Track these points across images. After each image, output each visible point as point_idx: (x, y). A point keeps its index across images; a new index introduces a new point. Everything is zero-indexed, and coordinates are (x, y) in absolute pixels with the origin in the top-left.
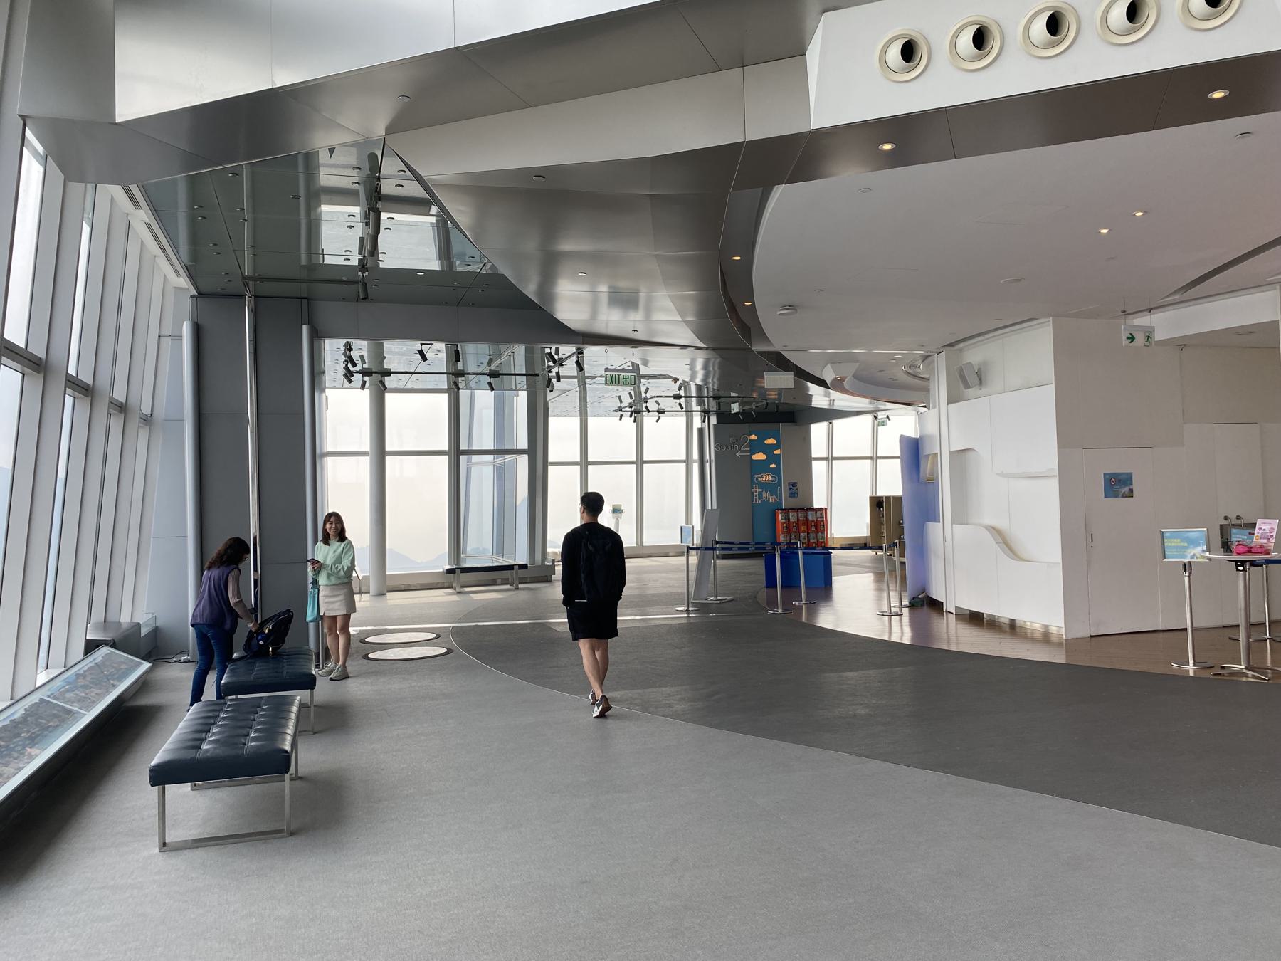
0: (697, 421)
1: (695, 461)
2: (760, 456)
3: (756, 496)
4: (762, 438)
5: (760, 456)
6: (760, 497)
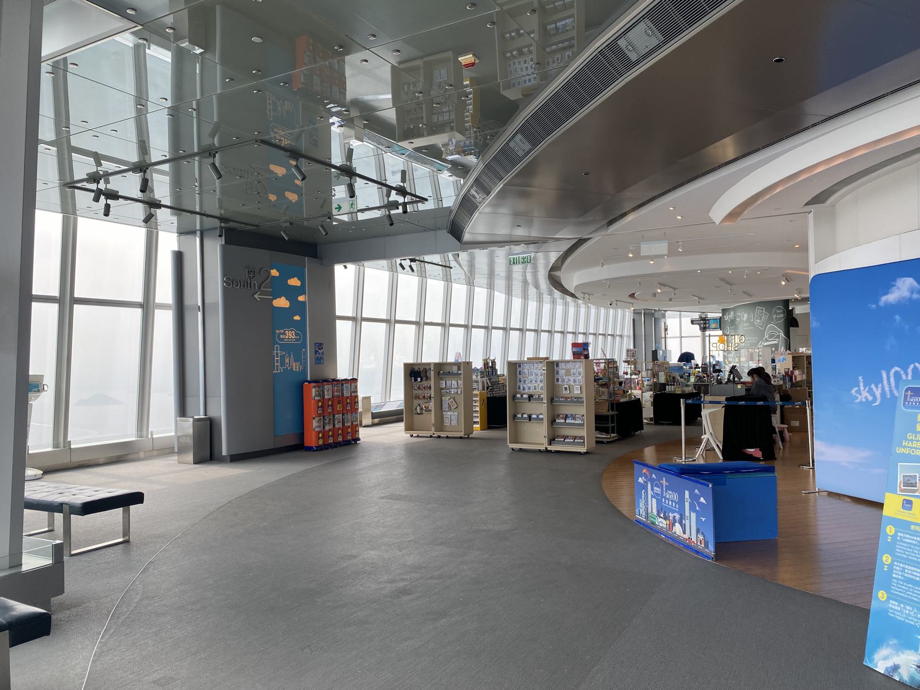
1: (163, 306)
2: (282, 302)
4: (285, 276)
5: (282, 302)
6: (283, 364)
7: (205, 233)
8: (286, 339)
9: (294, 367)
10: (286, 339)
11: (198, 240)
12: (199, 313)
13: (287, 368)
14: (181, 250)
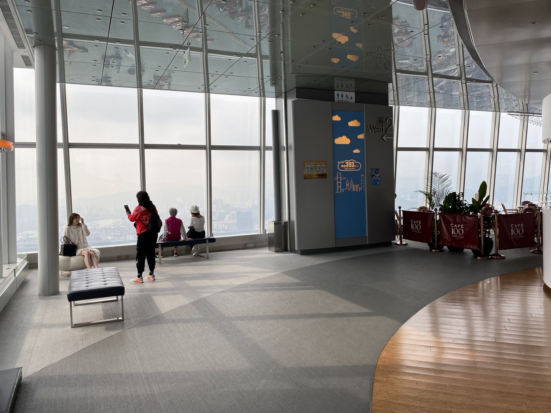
0: (271, 103)
2: (343, 140)
3: (339, 184)
4: (345, 120)
5: (343, 140)
6: (344, 186)
7: (287, 94)
8: (346, 168)
9: (353, 188)
10: (346, 168)
11: (283, 99)
12: (285, 151)
14: (277, 109)
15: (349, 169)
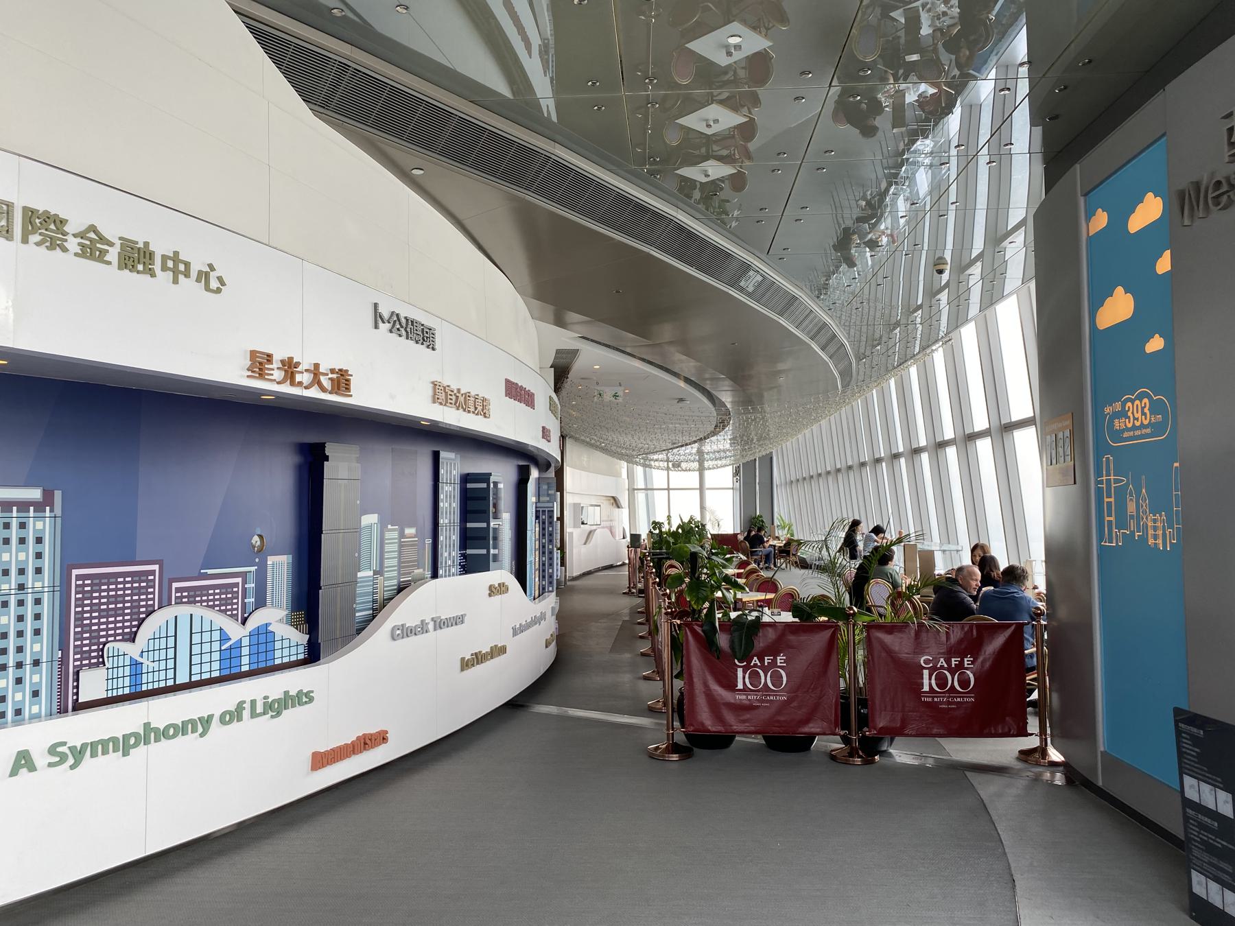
8: (1129, 430)
13: (1133, 533)
15: (1144, 431)
